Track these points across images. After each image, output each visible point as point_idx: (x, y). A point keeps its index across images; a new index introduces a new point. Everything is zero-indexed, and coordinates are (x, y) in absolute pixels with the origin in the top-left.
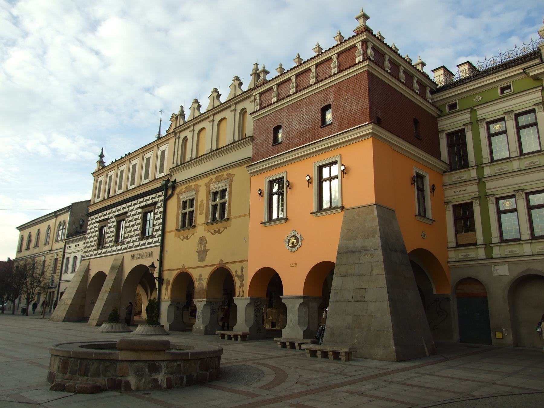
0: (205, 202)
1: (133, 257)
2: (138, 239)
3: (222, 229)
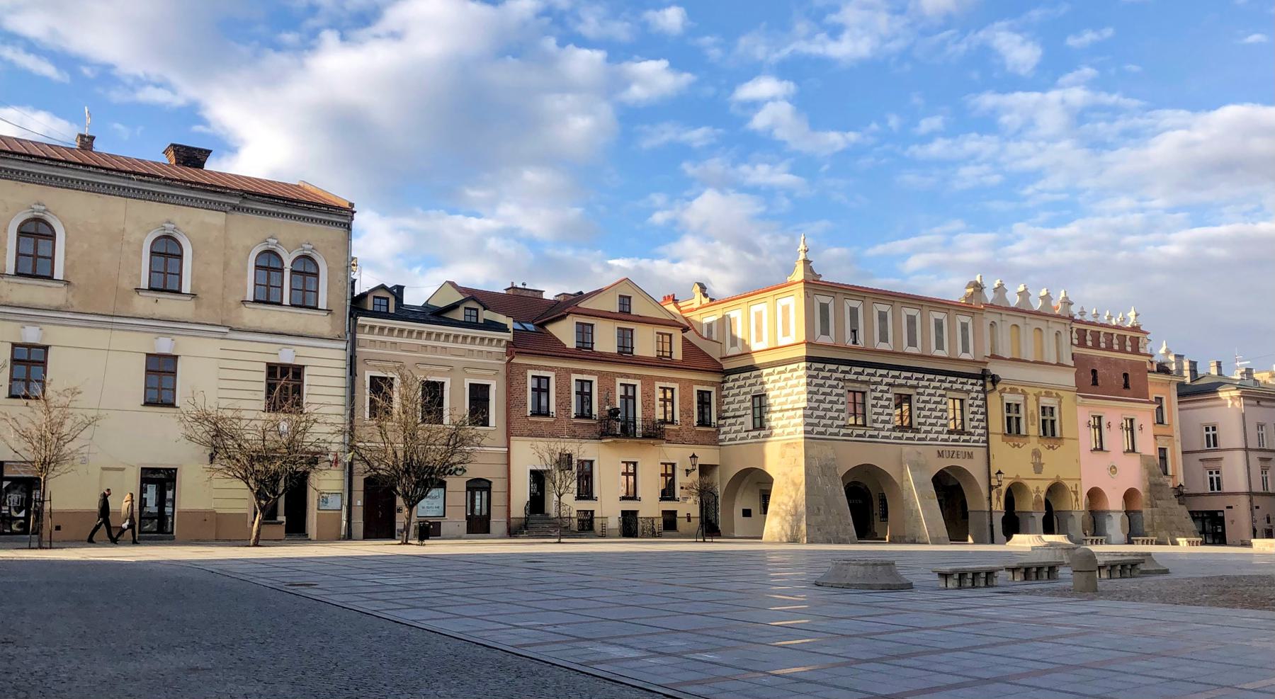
0: (1035, 412)
1: (940, 454)
2: (945, 432)
3: (1055, 447)
